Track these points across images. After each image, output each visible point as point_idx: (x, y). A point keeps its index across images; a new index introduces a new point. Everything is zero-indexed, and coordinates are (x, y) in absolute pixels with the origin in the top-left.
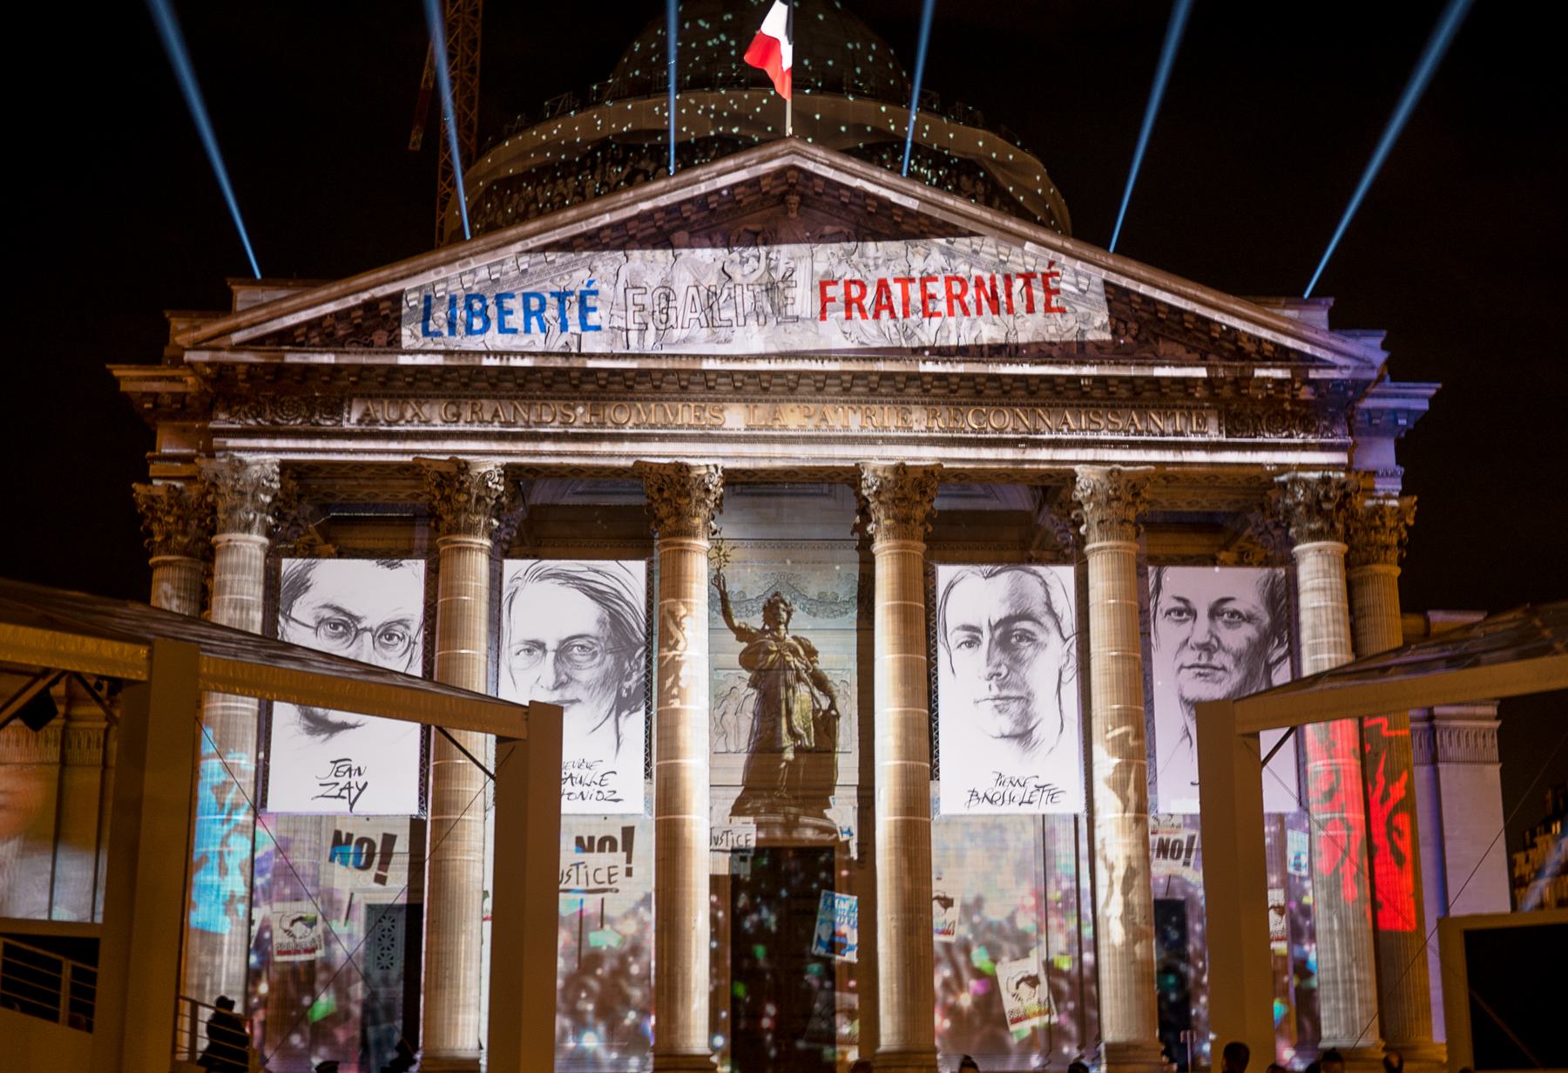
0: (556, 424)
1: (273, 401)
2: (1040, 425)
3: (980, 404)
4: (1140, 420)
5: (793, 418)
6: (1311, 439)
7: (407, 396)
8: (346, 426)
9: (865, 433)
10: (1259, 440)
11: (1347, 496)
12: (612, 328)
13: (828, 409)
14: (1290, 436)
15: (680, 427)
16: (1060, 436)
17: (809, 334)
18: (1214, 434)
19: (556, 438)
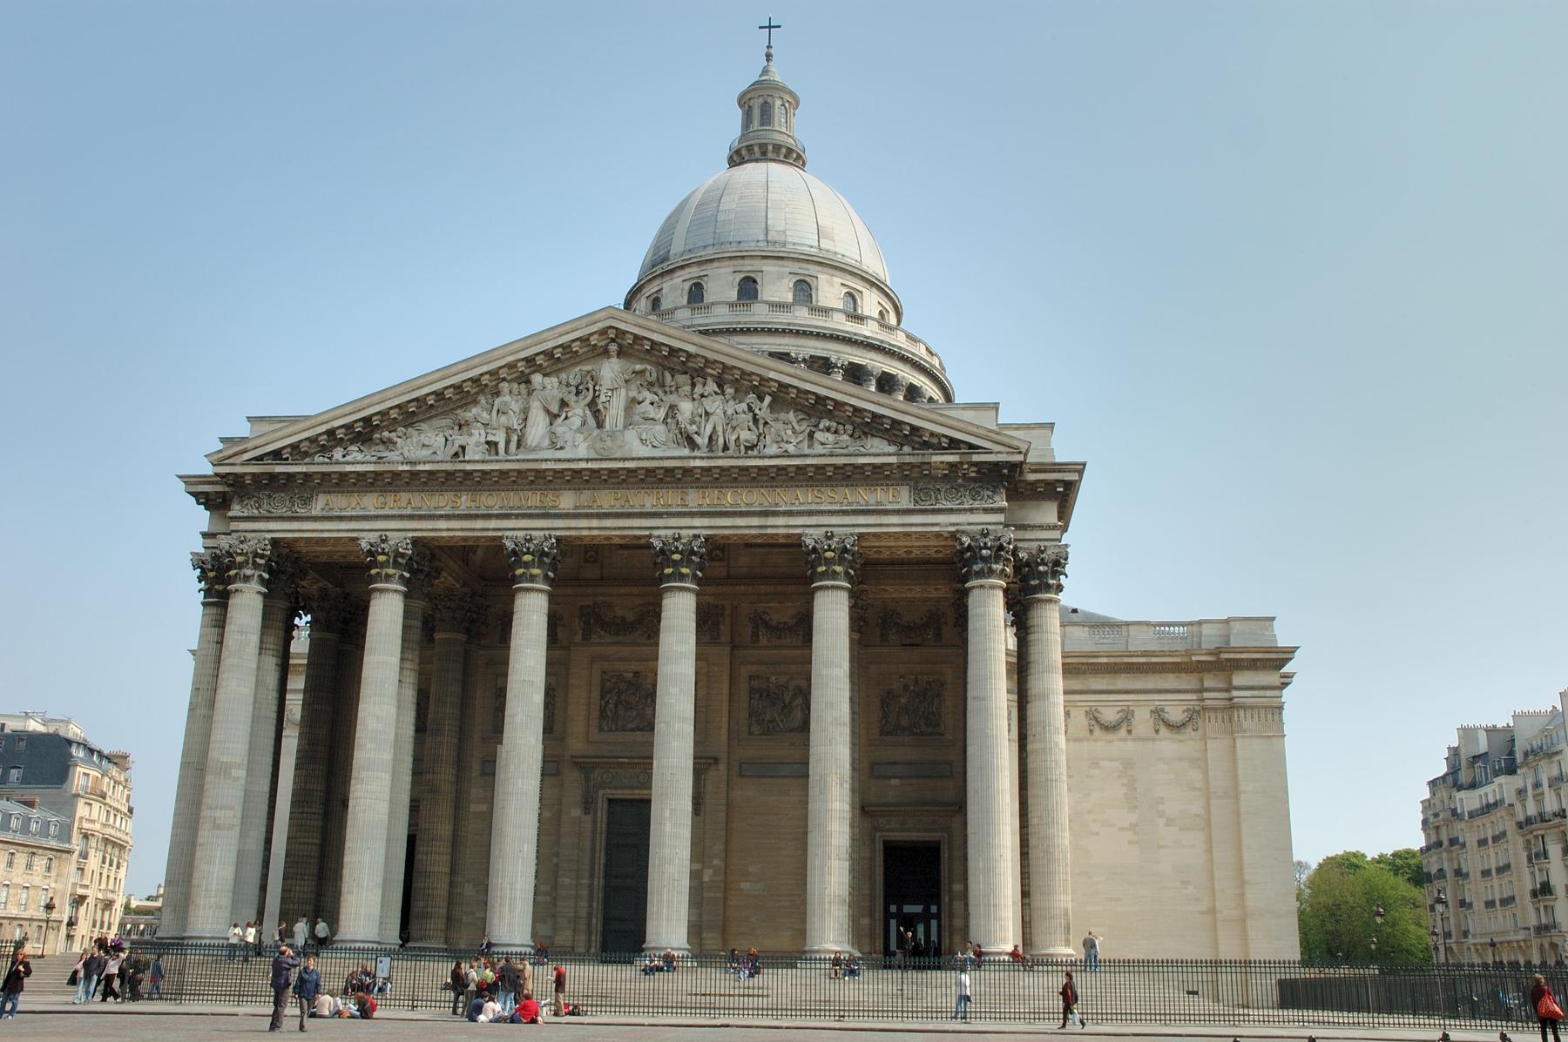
5: (607, 499)
6: (976, 505)
8: (314, 513)
12: (488, 443)
13: (630, 493)
17: (619, 443)
19: (448, 517)
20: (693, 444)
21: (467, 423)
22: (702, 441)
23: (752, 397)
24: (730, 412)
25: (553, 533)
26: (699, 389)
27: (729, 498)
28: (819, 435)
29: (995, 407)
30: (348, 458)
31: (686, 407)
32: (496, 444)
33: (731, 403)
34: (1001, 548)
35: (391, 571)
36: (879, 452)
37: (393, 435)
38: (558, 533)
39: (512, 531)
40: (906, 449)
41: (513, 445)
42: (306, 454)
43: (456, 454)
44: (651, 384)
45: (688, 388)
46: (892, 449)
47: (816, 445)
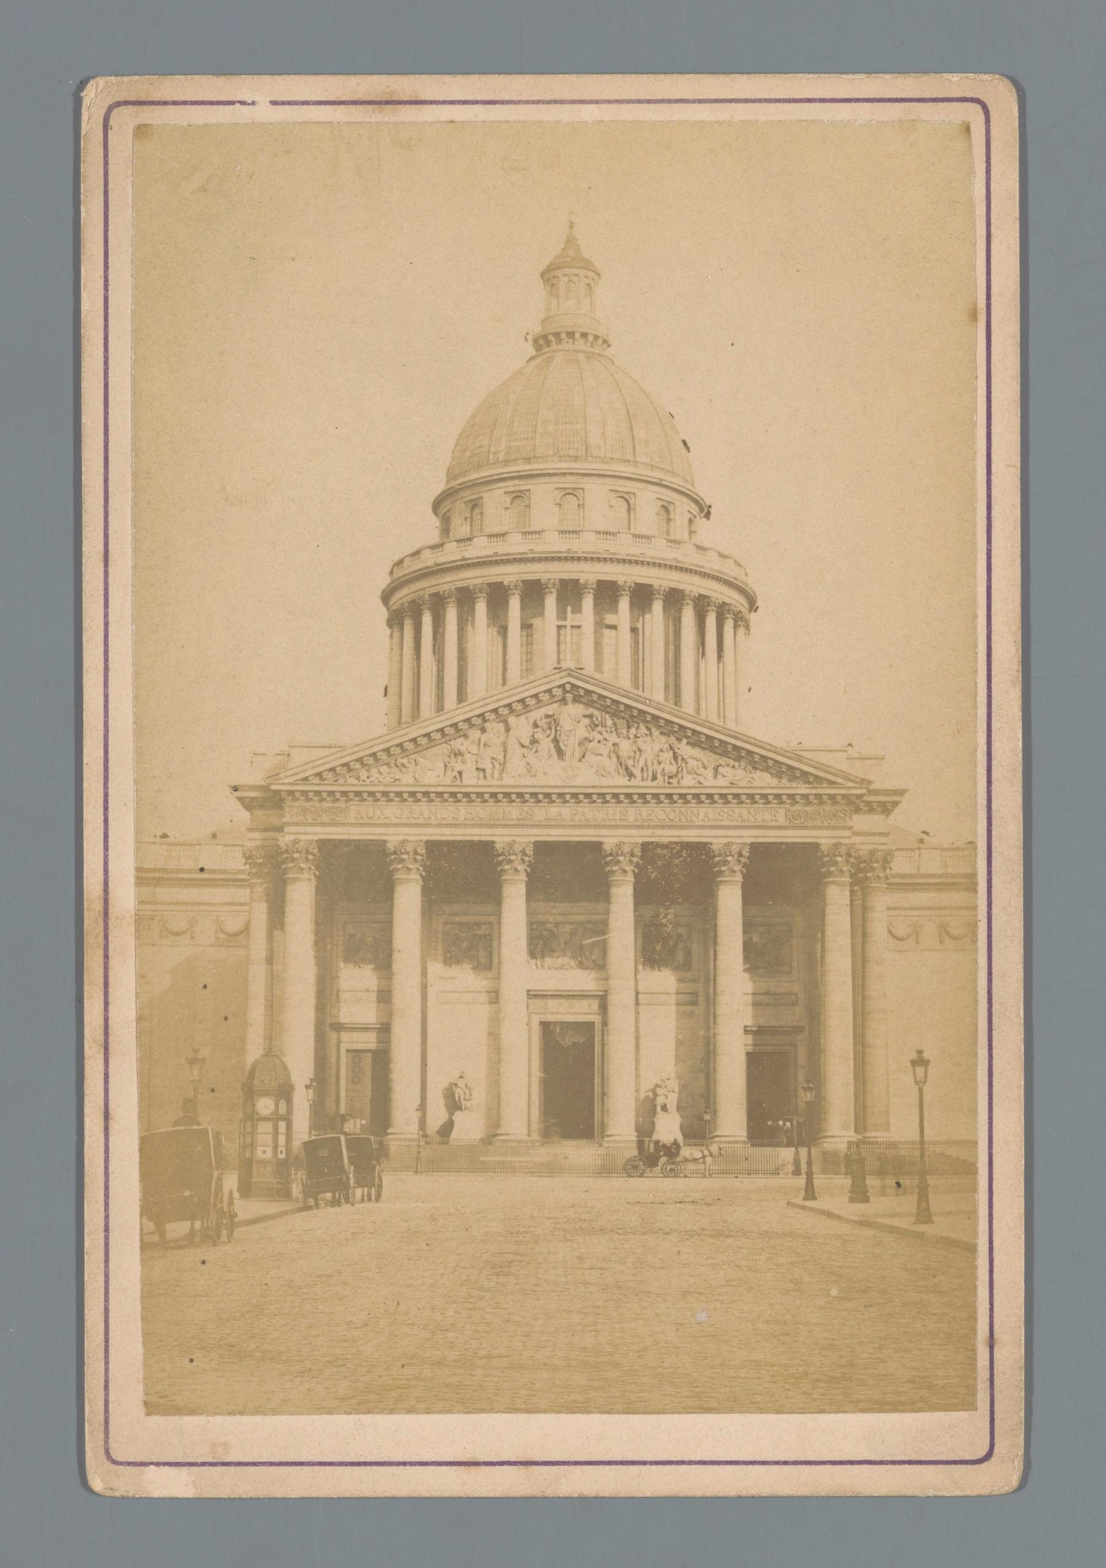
8: (349, 821)
12: (477, 769)
13: (586, 810)
18: (782, 821)
20: (631, 775)
21: (460, 754)
22: (637, 772)
23: (672, 739)
26: (633, 731)
28: (721, 769)
31: (625, 746)
32: (484, 770)
34: (849, 855)
39: (500, 838)
40: (785, 781)
45: (624, 731)
46: (774, 781)
47: (720, 776)
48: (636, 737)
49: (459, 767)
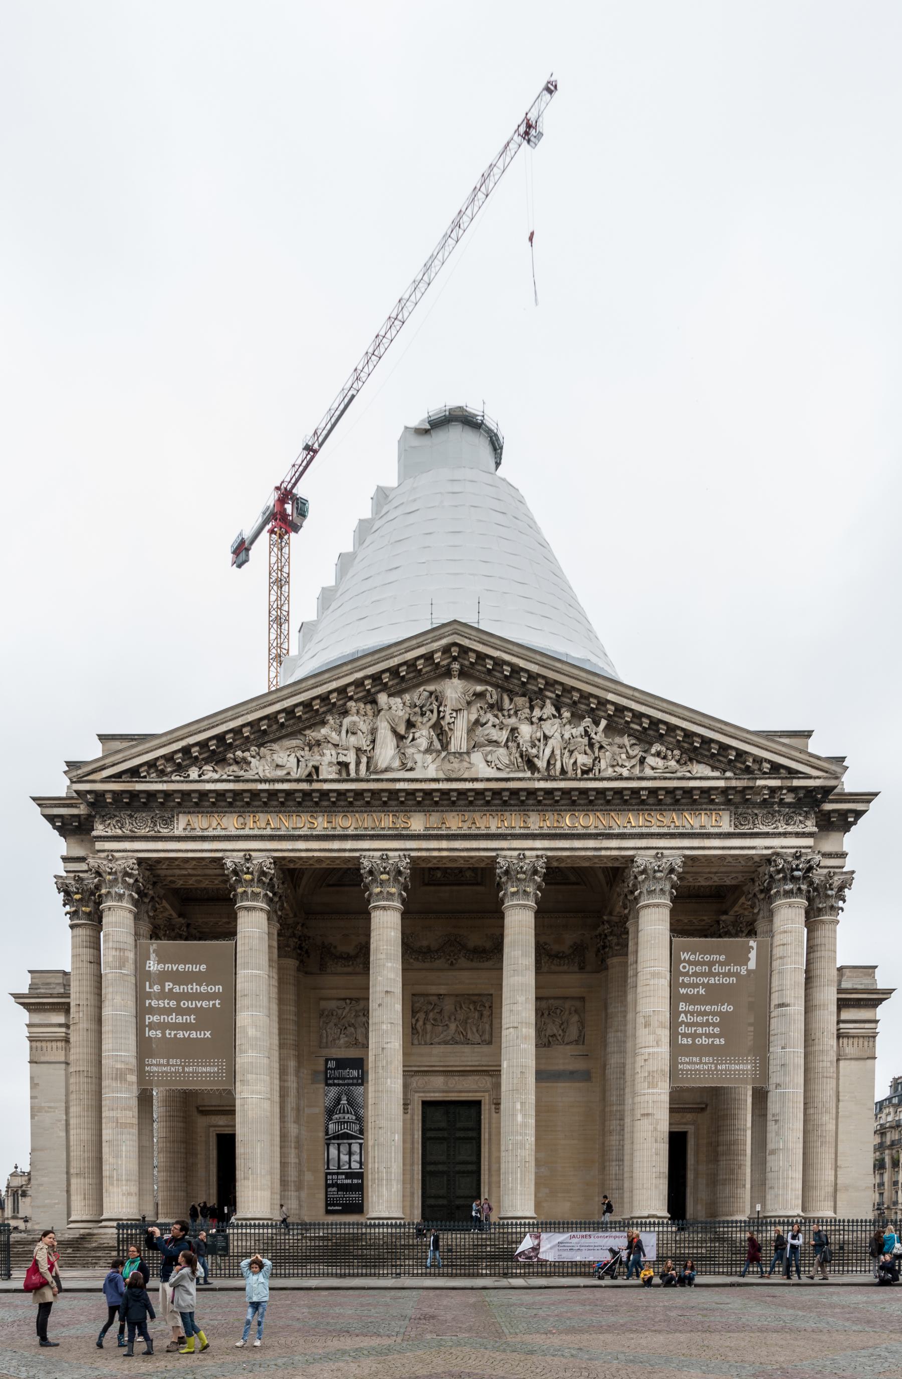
0: (305, 829)
1: (131, 816)
2: (612, 823)
3: (574, 810)
4: (678, 818)
5: (454, 822)
6: (790, 829)
7: (212, 812)
9: (500, 831)
10: (756, 830)
11: (810, 869)
12: (339, 763)
13: (477, 816)
14: (776, 828)
15: (383, 829)
16: (625, 831)
19: (306, 838)
22: (541, 764)
24: (567, 736)
25: (407, 853)
26: (537, 713)
27: (567, 822)
29: (808, 734)
30: (203, 777)
33: (568, 727)
35: (258, 890)
36: (703, 776)
37: (247, 754)
38: (413, 854)
39: (369, 852)
40: (729, 774)
41: (363, 767)
42: (162, 773)
43: (310, 775)
44: (491, 706)
46: (717, 774)
48: (541, 719)
49: (315, 759)
